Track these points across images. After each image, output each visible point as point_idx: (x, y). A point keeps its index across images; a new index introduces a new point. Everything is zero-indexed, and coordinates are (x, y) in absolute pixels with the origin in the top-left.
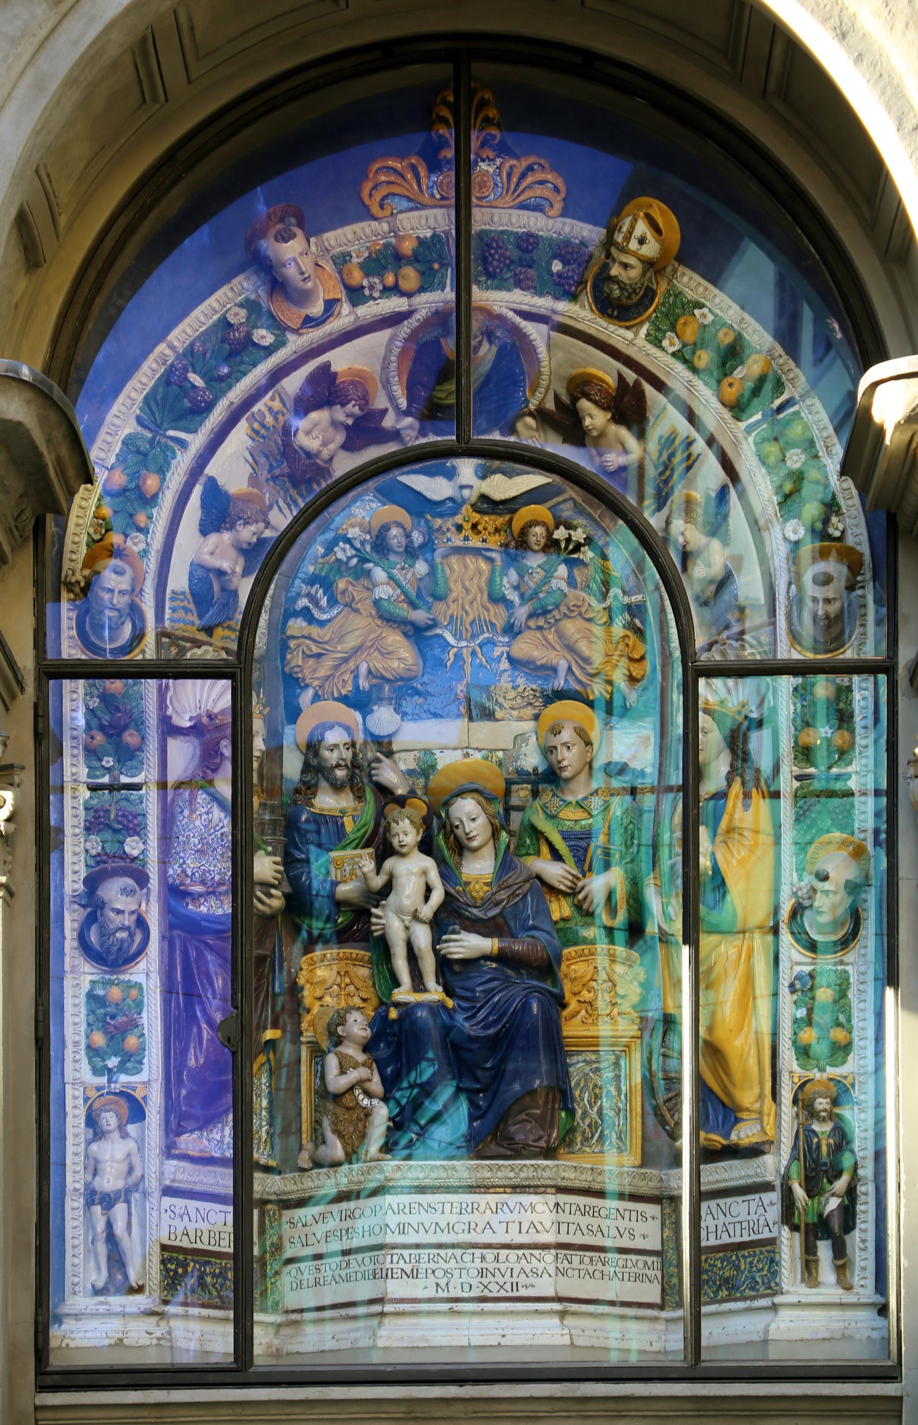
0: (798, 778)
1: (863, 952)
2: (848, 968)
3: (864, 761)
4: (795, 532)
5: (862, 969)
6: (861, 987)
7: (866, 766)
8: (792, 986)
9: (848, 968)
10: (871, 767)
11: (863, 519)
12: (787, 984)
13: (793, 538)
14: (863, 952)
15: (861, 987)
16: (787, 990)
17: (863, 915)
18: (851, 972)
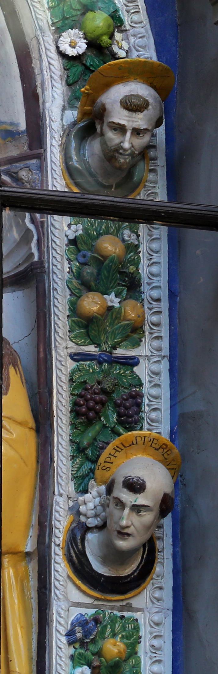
0: (74, 357)
1: (157, 594)
2: (137, 615)
3: (156, 343)
4: (73, 45)
5: (156, 618)
6: (156, 643)
7: (159, 349)
8: (70, 634)
9: (137, 615)
10: (166, 351)
11: (152, 41)
12: (63, 631)
13: (71, 52)
14: (157, 594)
15: (156, 643)
16: (64, 639)
17: (159, 544)
18: (141, 622)
